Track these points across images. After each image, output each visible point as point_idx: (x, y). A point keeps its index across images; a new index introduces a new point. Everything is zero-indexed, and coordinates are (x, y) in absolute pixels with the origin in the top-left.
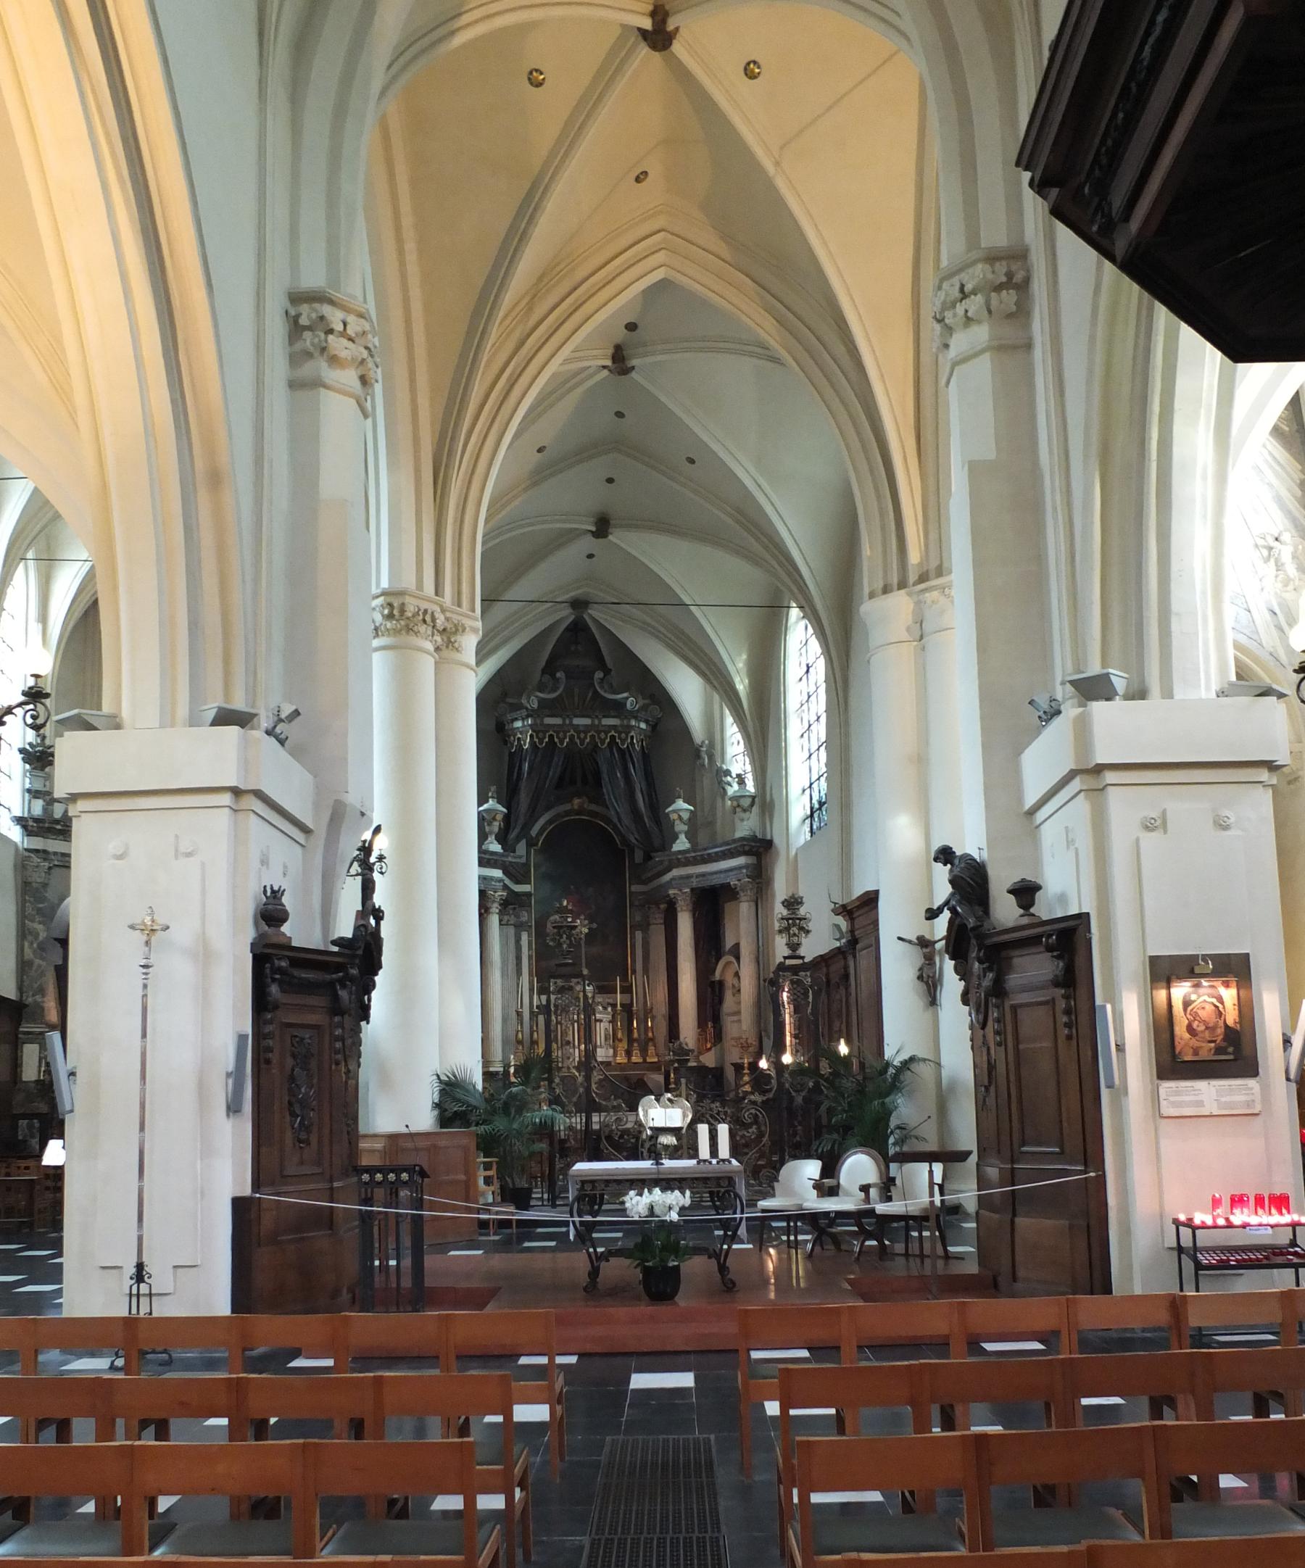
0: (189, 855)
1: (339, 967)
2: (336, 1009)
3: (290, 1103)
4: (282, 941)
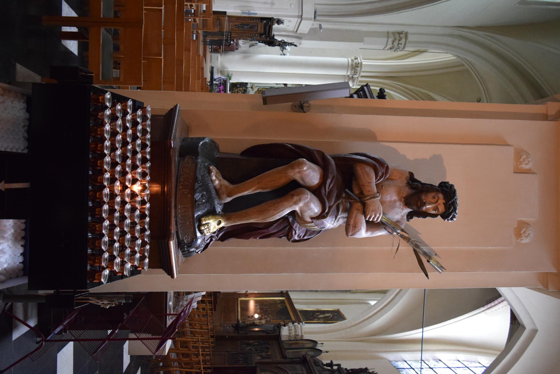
0: (290, 6)
1: (269, 36)
2: (261, 35)
3: (243, 24)
4: (274, 24)
